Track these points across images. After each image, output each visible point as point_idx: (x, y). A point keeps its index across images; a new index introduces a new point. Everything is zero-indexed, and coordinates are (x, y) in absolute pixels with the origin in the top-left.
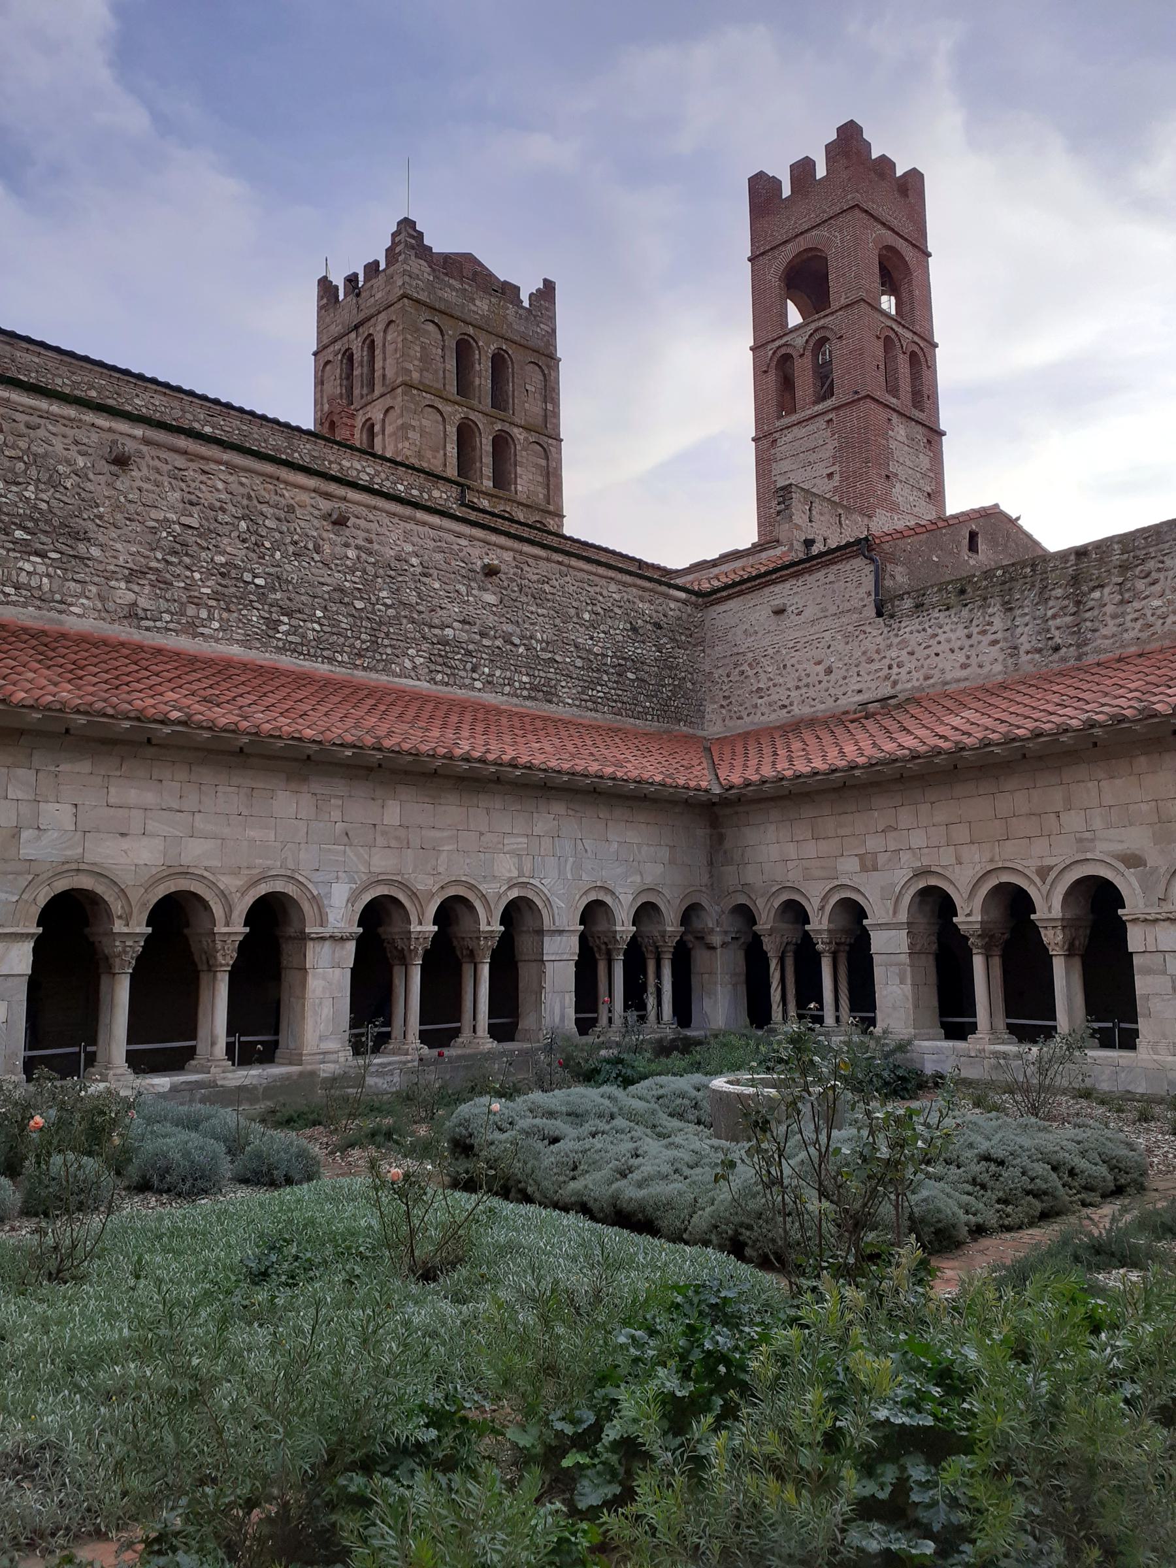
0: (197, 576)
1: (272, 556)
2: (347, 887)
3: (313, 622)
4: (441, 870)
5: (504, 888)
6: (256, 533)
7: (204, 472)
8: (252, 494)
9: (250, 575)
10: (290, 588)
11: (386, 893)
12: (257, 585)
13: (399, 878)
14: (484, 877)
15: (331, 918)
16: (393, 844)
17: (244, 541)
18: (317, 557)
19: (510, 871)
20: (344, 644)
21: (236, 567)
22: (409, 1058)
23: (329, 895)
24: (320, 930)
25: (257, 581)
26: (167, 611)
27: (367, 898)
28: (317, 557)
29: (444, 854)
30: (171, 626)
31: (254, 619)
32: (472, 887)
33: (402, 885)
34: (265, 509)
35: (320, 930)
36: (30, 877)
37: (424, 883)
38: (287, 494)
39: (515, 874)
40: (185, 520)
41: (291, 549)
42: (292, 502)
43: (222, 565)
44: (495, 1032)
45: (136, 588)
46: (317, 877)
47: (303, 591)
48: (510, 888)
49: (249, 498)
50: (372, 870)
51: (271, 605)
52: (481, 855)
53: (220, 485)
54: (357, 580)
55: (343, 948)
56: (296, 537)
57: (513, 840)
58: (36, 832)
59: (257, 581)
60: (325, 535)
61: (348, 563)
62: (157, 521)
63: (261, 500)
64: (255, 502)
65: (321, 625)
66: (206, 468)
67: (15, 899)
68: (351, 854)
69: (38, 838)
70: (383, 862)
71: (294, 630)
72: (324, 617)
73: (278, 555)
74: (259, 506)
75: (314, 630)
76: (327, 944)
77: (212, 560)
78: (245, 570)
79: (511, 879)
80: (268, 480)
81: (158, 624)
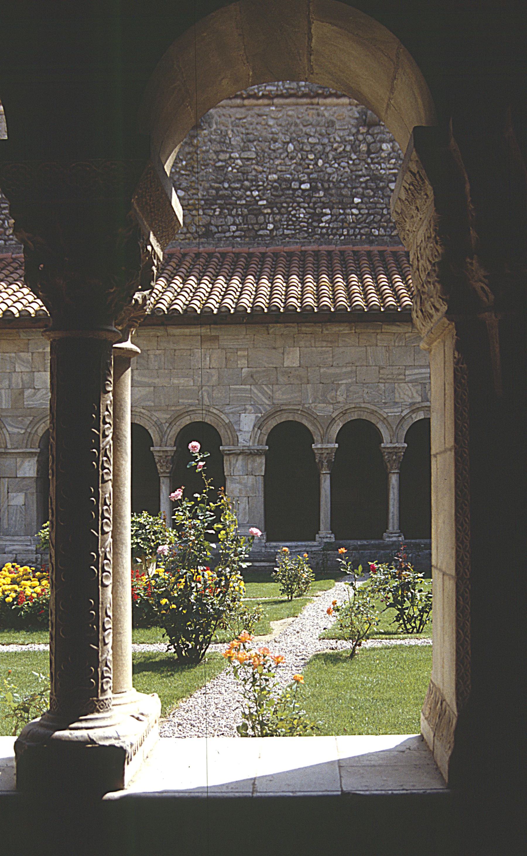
0: (256, 193)
1: (316, 164)
2: (253, 416)
3: (351, 208)
4: (341, 399)
5: (405, 413)
6: (302, 149)
7: (259, 115)
8: (298, 121)
9: (297, 183)
10: (331, 185)
11: (291, 419)
12: (304, 191)
13: (300, 407)
14: (385, 403)
15: (240, 440)
16: (296, 382)
17: (292, 159)
18: (354, 157)
19: (413, 397)
20: (380, 220)
21: (285, 180)
22: (315, 543)
23: (238, 422)
24: (232, 448)
25: (303, 187)
26: (234, 224)
27: (272, 423)
28: (354, 157)
29: (343, 387)
30: (237, 233)
31: (302, 216)
32: (373, 412)
33: (308, 413)
34: (307, 130)
35: (232, 448)
36: (31, 418)
37: (323, 410)
38: (326, 114)
39: (419, 399)
40: (245, 155)
41: (331, 156)
42: (333, 118)
43: (275, 181)
44: (403, 528)
45: (211, 212)
46: (227, 409)
47: (342, 185)
48: (413, 411)
49: (296, 125)
50: (275, 402)
51: (315, 203)
52: (382, 385)
53: (271, 122)
54: (392, 166)
55: (254, 461)
56: (335, 145)
57: (416, 371)
58: (33, 390)
59: (303, 187)
60: (361, 137)
61: (383, 155)
62: (225, 161)
63: (305, 124)
64: (301, 126)
65: (359, 209)
66: (261, 112)
67: (23, 431)
68: (256, 391)
69: (34, 394)
70: (281, 396)
71: (335, 218)
72: (362, 202)
73: (320, 162)
74: (304, 129)
75: (352, 214)
76: (240, 457)
77: (267, 178)
78: (293, 180)
79: (414, 403)
80: (311, 107)
81: (228, 234)
